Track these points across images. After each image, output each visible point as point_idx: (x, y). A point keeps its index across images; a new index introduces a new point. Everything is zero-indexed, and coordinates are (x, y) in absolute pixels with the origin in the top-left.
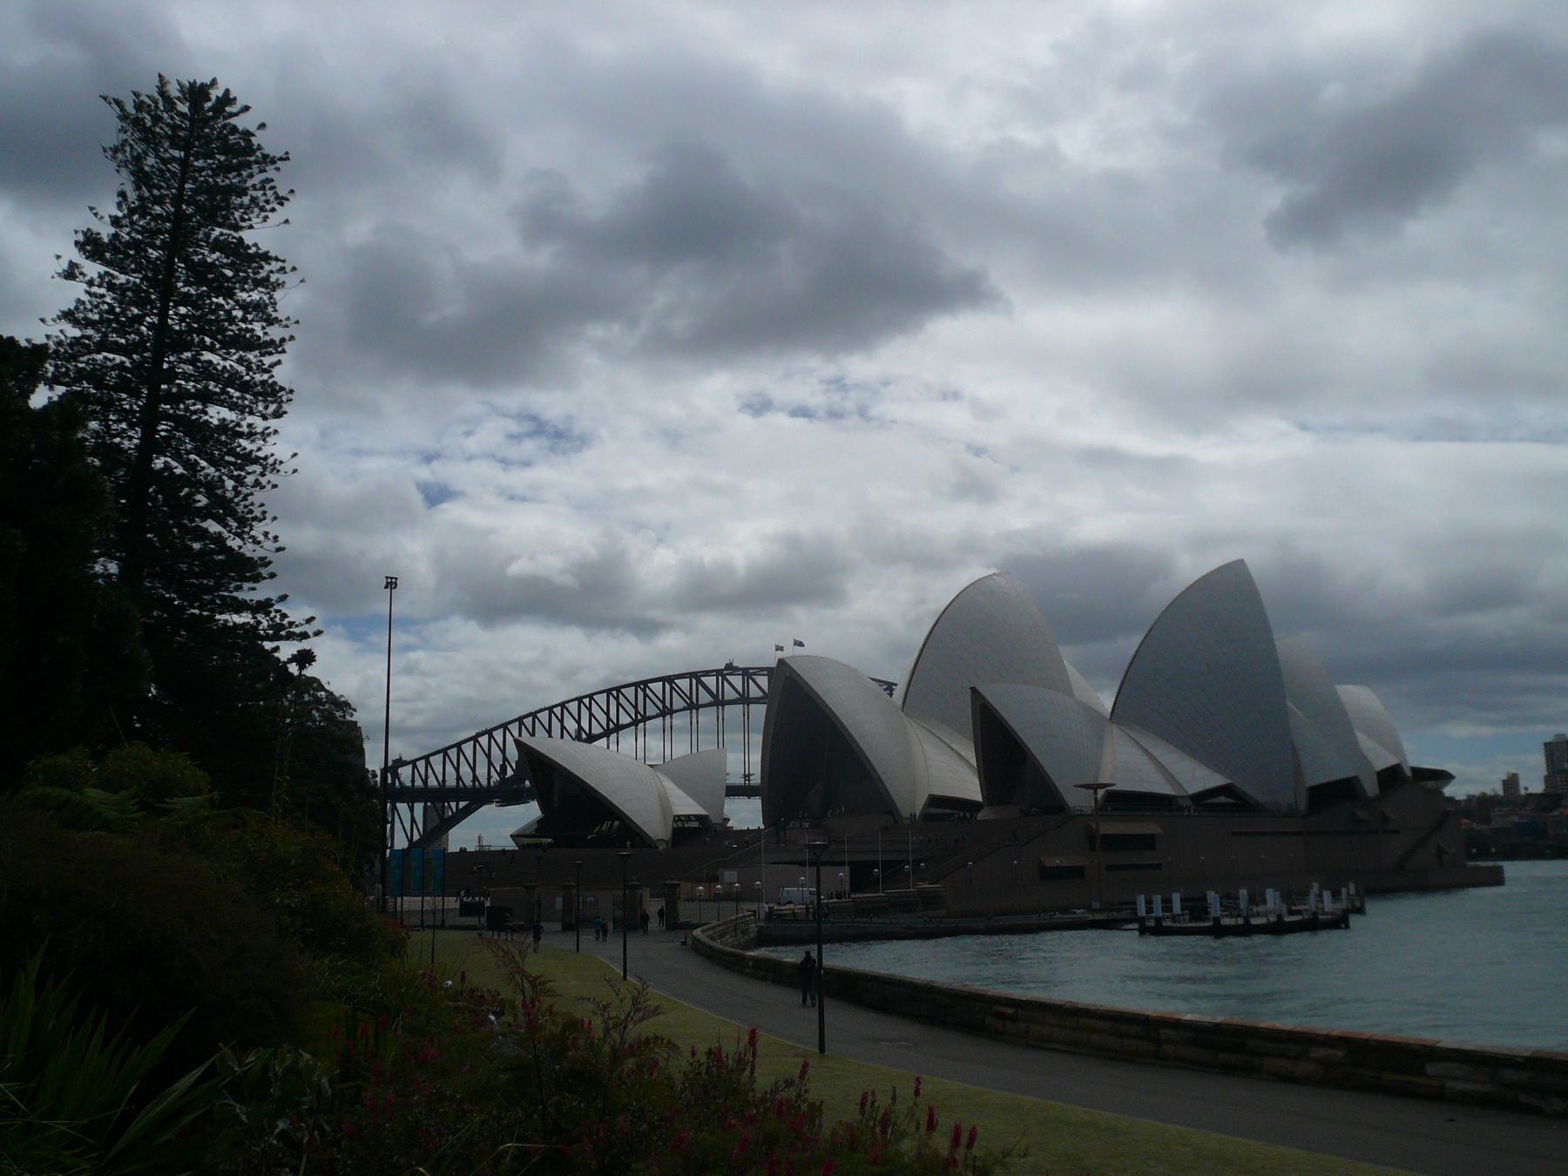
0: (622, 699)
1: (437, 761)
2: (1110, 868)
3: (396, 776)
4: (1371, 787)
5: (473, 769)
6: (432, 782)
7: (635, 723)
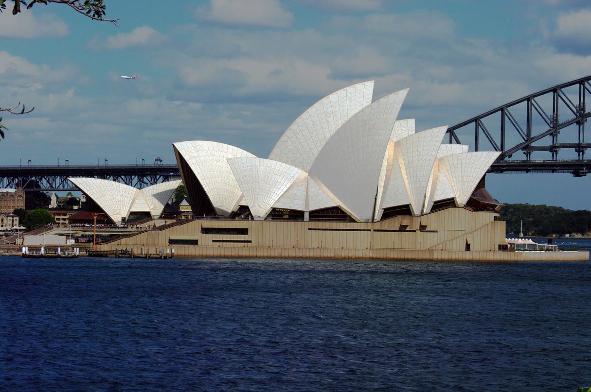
2: (214, 241)
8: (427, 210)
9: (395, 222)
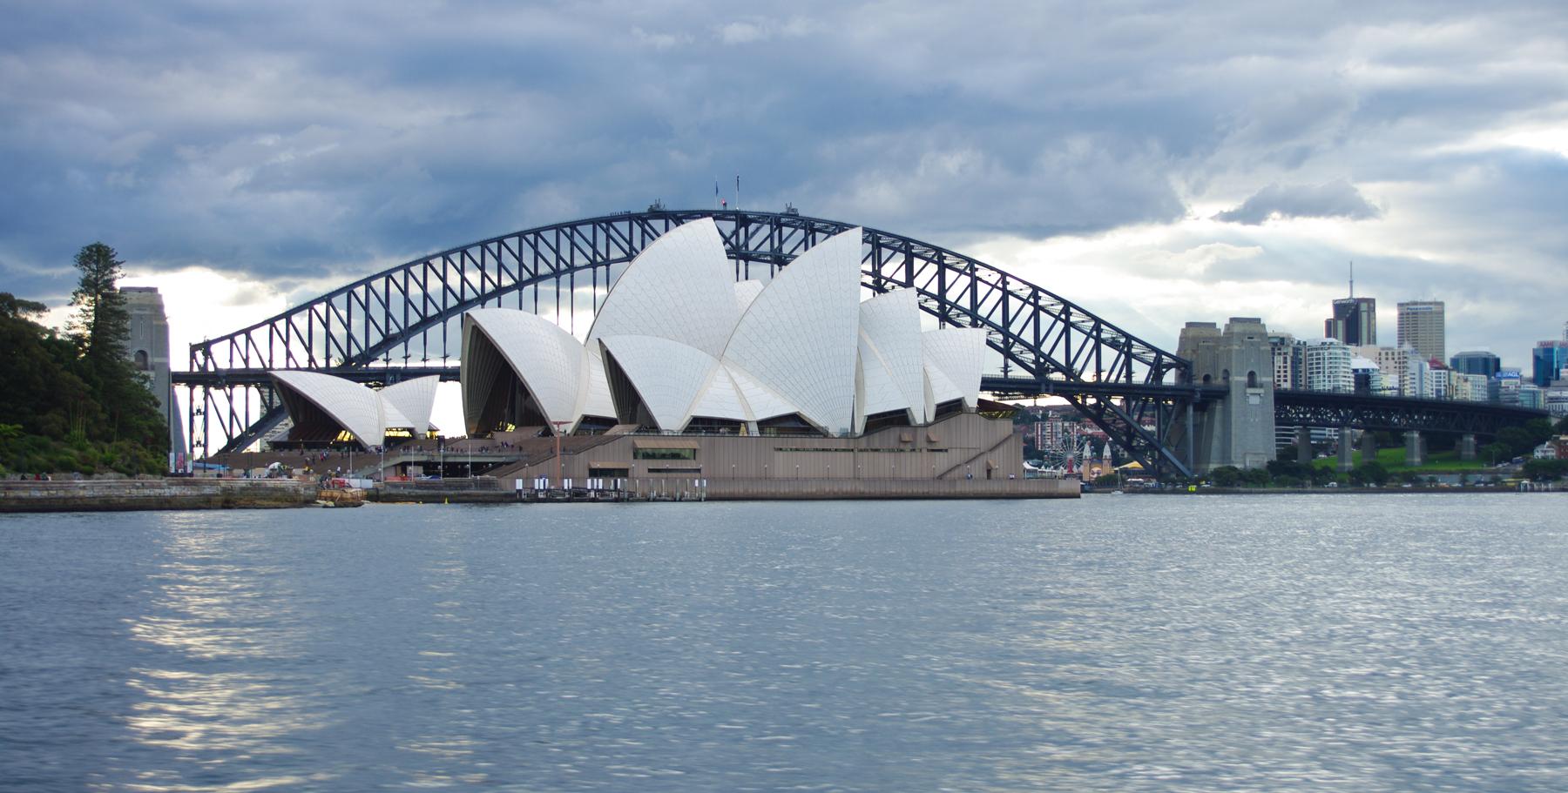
0: (542, 246)
1: (261, 335)
2: (650, 471)
3: (207, 354)
4: (921, 413)
5: (348, 326)
6: (255, 364)
7: (557, 273)
8: (930, 418)
9: (891, 435)
